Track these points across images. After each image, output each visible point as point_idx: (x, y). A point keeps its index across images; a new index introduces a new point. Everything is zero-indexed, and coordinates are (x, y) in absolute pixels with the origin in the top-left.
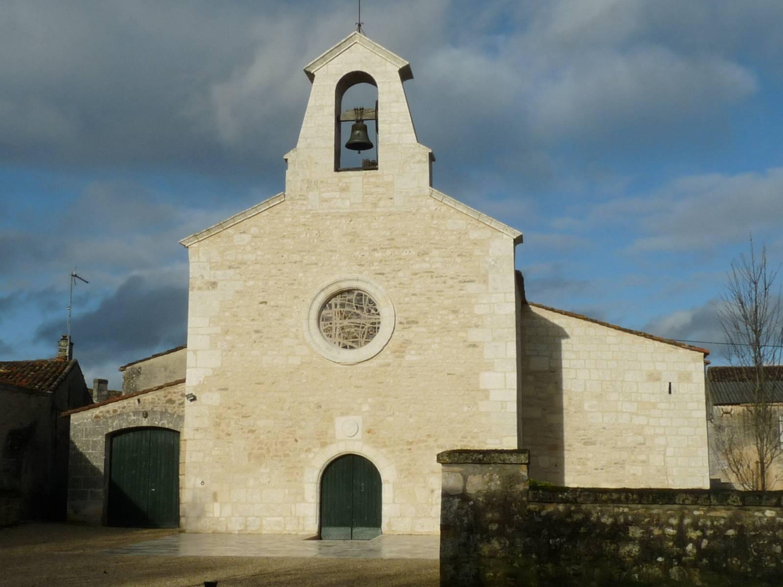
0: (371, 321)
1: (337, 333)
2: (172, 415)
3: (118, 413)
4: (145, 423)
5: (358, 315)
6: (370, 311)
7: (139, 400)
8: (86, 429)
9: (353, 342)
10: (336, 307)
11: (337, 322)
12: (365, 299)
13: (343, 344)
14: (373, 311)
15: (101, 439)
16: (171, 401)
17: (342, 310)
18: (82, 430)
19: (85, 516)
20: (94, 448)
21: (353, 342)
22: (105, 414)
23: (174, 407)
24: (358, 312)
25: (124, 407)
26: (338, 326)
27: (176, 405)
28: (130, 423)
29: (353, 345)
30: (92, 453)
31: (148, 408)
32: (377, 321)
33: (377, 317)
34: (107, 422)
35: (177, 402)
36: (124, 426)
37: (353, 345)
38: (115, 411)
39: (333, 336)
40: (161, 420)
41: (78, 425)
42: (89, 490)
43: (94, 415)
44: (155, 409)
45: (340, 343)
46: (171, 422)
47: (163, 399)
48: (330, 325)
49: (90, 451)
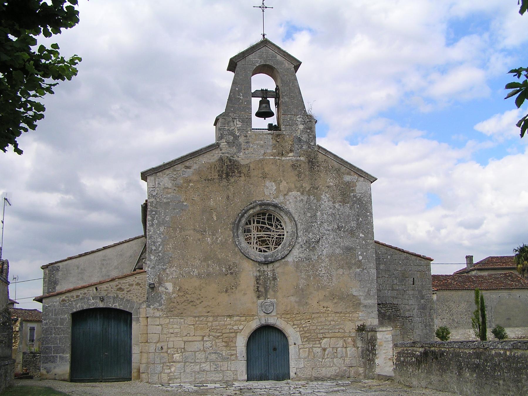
0: (278, 233)
1: (255, 241)
2: (122, 299)
3: (81, 297)
4: (101, 305)
5: (269, 229)
6: (277, 227)
7: (96, 288)
8: (55, 310)
9: (266, 248)
10: (254, 223)
11: (255, 234)
12: (274, 218)
13: (259, 249)
14: (279, 227)
15: (67, 317)
16: (120, 289)
17: (258, 225)
18: (52, 310)
19: (55, 374)
20: (62, 324)
21: (266, 248)
22: (70, 298)
23: (124, 294)
24: (269, 227)
25: (85, 294)
26: (256, 236)
27: (125, 292)
28: (90, 305)
29: (266, 250)
30: (61, 328)
31: (104, 294)
32: (282, 233)
33: (282, 231)
34: (72, 304)
35: (126, 290)
36: (85, 307)
37: (266, 250)
38: (78, 296)
39: (252, 243)
40: (114, 303)
41: (49, 306)
42: (58, 355)
43: (61, 299)
44: (109, 295)
45: (257, 248)
46: (121, 305)
47: (115, 287)
48: (250, 236)
49: (59, 326)
